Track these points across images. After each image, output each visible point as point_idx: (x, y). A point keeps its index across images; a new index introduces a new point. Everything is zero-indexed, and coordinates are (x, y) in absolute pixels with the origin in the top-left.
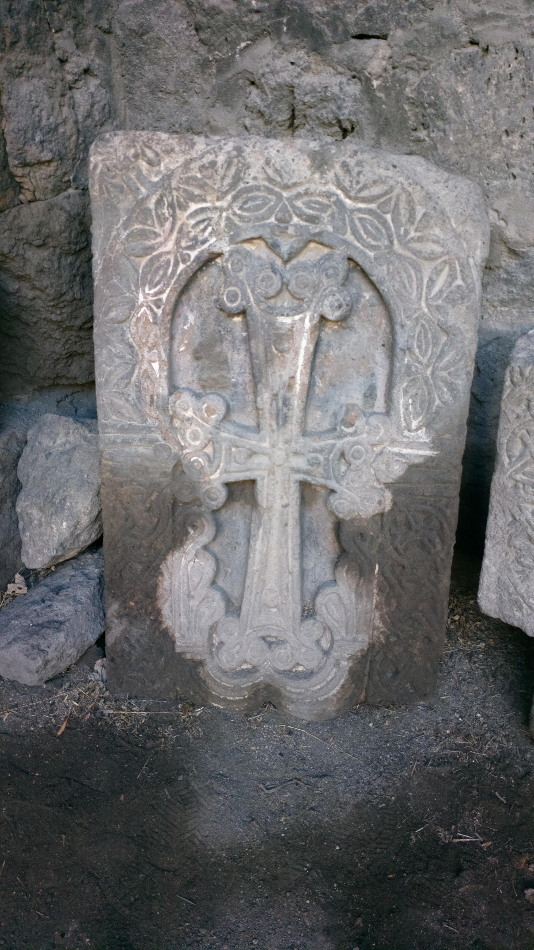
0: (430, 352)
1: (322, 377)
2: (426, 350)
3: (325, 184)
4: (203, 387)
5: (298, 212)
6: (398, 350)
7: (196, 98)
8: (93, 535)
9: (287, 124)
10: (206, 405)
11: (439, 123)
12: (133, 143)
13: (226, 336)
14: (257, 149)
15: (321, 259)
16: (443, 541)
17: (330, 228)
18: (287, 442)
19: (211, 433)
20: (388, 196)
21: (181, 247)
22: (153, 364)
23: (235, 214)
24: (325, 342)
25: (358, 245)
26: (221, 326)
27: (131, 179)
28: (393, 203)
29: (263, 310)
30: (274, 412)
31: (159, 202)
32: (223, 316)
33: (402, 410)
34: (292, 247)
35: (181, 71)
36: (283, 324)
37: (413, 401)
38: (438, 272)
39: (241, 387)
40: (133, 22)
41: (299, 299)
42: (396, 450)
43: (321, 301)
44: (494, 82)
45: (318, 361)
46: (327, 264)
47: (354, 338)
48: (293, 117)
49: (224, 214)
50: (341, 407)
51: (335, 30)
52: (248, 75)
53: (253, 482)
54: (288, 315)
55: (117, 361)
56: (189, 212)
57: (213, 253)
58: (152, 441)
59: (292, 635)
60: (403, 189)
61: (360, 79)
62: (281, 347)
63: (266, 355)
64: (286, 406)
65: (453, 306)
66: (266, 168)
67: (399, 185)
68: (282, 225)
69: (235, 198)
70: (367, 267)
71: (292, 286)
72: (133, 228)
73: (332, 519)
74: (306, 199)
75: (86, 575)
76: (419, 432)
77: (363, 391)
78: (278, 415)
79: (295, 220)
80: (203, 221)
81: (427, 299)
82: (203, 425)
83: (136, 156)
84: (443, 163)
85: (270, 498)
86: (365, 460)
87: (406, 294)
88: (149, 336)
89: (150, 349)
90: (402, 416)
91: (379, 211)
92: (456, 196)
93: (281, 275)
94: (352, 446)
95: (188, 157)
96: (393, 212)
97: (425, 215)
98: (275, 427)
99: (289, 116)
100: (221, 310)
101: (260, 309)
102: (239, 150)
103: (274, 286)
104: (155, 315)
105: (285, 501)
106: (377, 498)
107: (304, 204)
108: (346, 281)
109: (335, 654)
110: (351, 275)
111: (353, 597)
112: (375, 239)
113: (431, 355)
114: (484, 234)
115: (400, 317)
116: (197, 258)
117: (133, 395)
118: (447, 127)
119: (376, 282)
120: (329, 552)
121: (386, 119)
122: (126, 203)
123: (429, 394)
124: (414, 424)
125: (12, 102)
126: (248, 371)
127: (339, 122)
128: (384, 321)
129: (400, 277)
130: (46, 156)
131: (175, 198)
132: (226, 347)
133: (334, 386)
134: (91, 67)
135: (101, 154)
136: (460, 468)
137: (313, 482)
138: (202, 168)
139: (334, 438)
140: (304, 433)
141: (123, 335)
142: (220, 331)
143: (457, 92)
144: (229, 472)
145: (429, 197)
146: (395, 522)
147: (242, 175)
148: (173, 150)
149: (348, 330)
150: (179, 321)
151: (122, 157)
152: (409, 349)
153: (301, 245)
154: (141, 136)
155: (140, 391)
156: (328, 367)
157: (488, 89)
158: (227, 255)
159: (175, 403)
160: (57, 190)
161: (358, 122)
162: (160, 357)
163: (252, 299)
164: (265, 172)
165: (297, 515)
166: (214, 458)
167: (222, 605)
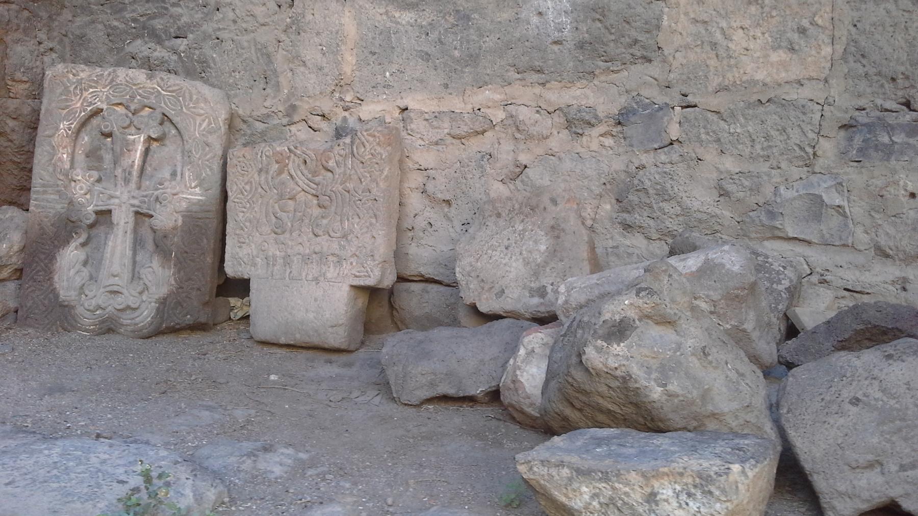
18: (129, 192)
31: (76, 87)
38: (204, 121)
40: (78, 32)
47: (167, 149)
51: (166, 36)
53: (110, 211)
58: (59, 191)
71: (135, 123)
84: (213, 85)
102: (114, 71)
108: (161, 124)
111: (160, 269)
115: (186, 137)
117: (51, 169)
125: (12, 53)
130: (25, 79)
132: (102, 152)
140: (139, 188)
150: (80, 139)
160: (28, 97)
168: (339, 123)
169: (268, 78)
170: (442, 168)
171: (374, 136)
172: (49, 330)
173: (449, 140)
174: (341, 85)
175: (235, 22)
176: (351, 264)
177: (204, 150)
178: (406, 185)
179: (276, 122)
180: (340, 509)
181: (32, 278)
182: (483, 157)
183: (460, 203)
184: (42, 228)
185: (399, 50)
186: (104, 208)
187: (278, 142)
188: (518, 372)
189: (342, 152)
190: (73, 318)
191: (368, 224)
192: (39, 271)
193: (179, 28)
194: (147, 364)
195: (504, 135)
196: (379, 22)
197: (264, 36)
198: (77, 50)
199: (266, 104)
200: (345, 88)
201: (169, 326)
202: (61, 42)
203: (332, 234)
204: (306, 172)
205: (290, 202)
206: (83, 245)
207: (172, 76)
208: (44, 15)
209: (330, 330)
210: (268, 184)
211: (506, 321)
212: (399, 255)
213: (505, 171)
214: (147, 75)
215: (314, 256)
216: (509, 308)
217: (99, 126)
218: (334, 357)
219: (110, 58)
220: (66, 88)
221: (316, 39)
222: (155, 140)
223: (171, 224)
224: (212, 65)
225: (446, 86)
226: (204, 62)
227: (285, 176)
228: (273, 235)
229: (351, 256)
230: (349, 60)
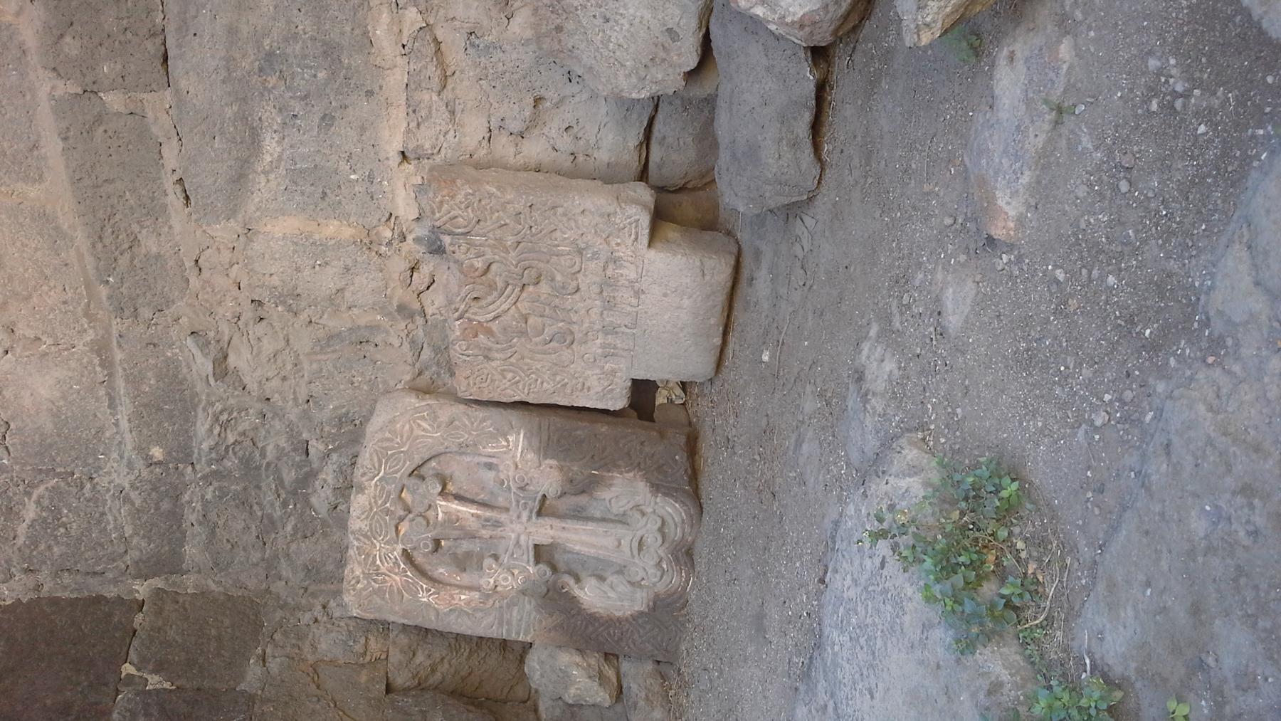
1: (477, 494)
3: (371, 487)
18: (511, 522)
31: (375, 581)
40: (302, 575)
47: (457, 473)
53: (536, 546)
58: (508, 606)
70: (414, 466)
71: (422, 510)
84: (371, 412)
102: (353, 533)
115: (442, 449)
130: (363, 640)
132: (459, 551)
140: (507, 510)
146: (565, 460)
160: (386, 637)
168: (423, 249)
169: (362, 340)
170: (488, 106)
171: (442, 202)
172: (683, 625)
173: (447, 94)
174: (369, 243)
175: (284, 379)
176: (618, 244)
177: (457, 428)
178: (512, 160)
179: (421, 333)
180: (951, 290)
181: (617, 642)
182: (472, 45)
183: (538, 84)
184: (555, 627)
185: (318, 159)
186: (532, 553)
187: (449, 332)
188: (789, 20)
189: (463, 248)
191: (565, 219)
192: (609, 634)
193: (294, 450)
194: (735, 511)
195: (442, 12)
196: (279, 184)
197: (303, 343)
198: (326, 576)
199: (396, 343)
200: (374, 238)
201: (688, 482)
202: (314, 595)
203: (577, 268)
204: (490, 299)
205: (531, 321)
206: (578, 580)
207: (360, 461)
208: (279, 614)
209: (708, 278)
210: (504, 349)
211: (712, 28)
212: (608, 177)
213: (494, 13)
214: (358, 493)
215: (605, 294)
216: (694, 23)
217: (425, 555)
218: (745, 273)
219: (336, 537)
220: (375, 592)
221: (307, 272)
222: (444, 486)
224: (344, 410)
225: (370, 93)
227: (495, 326)
228: (574, 346)
229: (608, 244)
230: (332, 229)
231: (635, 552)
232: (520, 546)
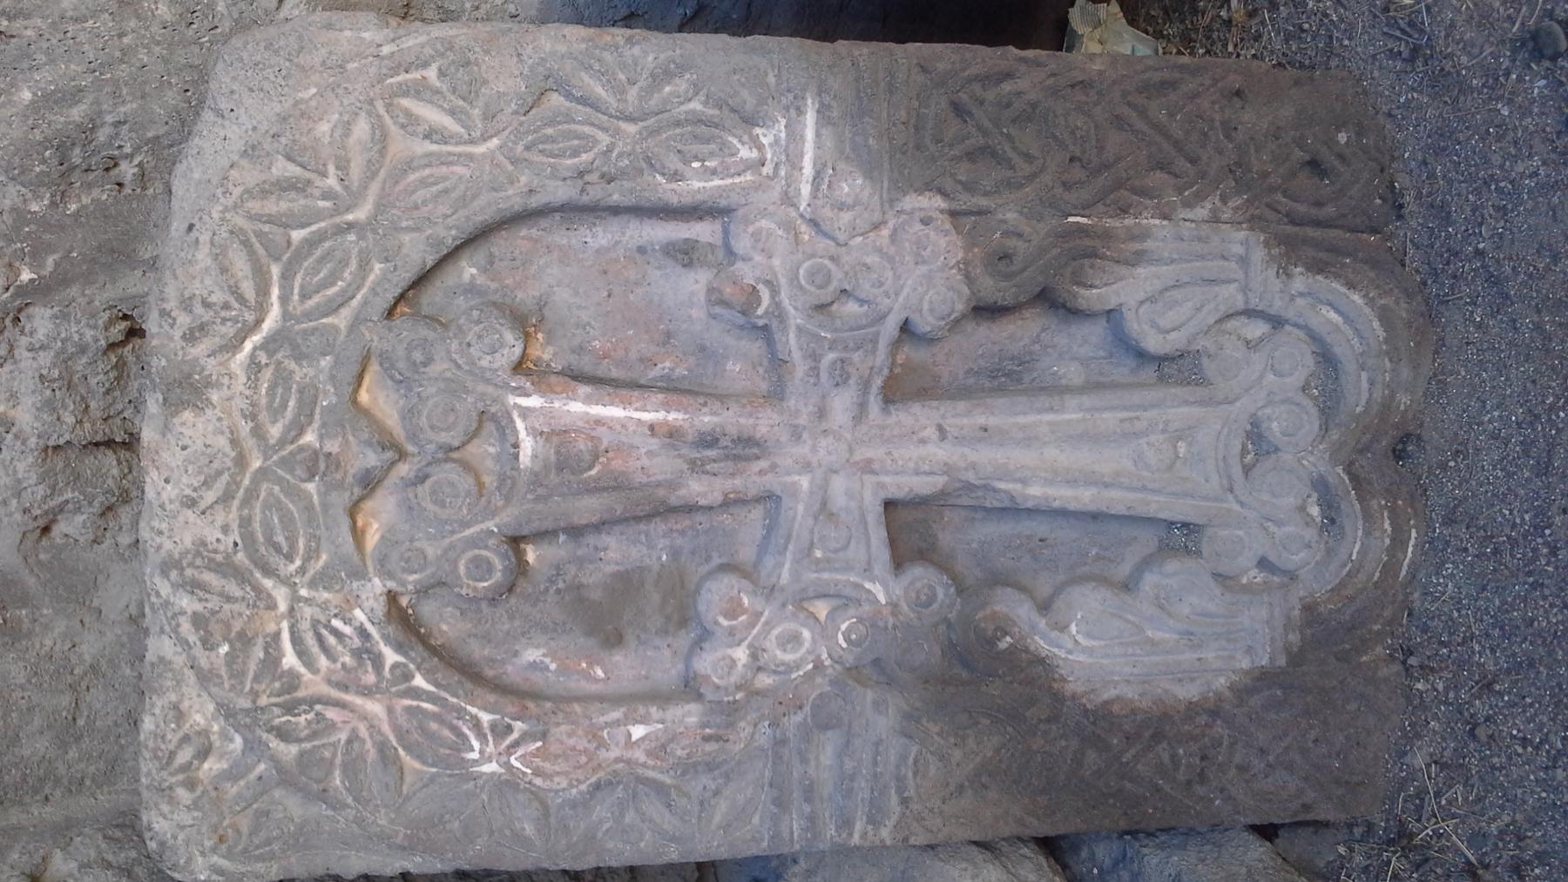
0: (587, 129)
2: (578, 137)
4: (683, 623)
5: (293, 433)
6: (585, 199)
7: (84, 648)
8: (1025, 851)
9: (123, 454)
10: (721, 620)
11: (102, 135)
12: (166, 792)
13: (568, 578)
14: (164, 526)
15: (392, 378)
16: (1009, 75)
17: (326, 362)
18: (796, 434)
19: (784, 605)
20: (254, 240)
21: (377, 686)
22: (634, 738)
23: (302, 570)
24: (573, 359)
25: (359, 297)
26: (547, 590)
27: (239, 795)
28: (266, 228)
29: (508, 499)
30: (729, 466)
31: (284, 734)
32: (523, 586)
33: (717, 182)
34: (368, 443)
35: (29, 681)
36: (535, 456)
37: (696, 158)
38: (410, 123)
39: (679, 541)
41: (480, 422)
42: (806, 190)
43: (483, 376)
44: (5, 23)
45: (615, 373)
46: (401, 365)
47: (562, 296)
48: (109, 443)
49: (304, 592)
50: (714, 317)
52: (29, 543)
53: (889, 505)
54: (516, 446)
55: (630, 817)
56: (303, 670)
57: (388, 614)
59: (1238, 404)
60: (236, 206)
61: (20, 310)
62: (588, 457)
63: (605, 489)
64: (717, 440)
65: (485, 82)
66: (203, 505)
67: (228, 216)
68: (322, 466)
69: (269, 571)
70: (407, 276)
72: (341, 788)
73: (969, 326)
74: (263, 417)
75: (1116, 864)
76: (765, 141)
77: (679, 269)
78: (737, 458)
79: (310, 438)
80: (320, 639)
81: (472, 142)
82: (766, 623)
83: (191, 785)
84: (184, 124)
85: (926, 468)
86: (832, 258)
87: (462, 187)
88: (573, 749)
89: (602, 744)
90: (729, 181)
91: (285, 258)
92: (251, 90)
93: (429, 464)
94: (801, 288)
95: (190, 676)
96: (286, 226)
97: (289, 158)
98: (763, 464)
99: (109, 453)
100: (511, 590)
101: (505, 507)
103: (454, 477)
104: (525, 738)
105: (931, 432)
106: (918, 227)
107: (274, 423)
109: (1278, 306)
110: (425, 310)
111: (1140, 270)
112: (344, 263)
113: (592, 124)
114: (329, 26)
115: (512, 198)
116: (399, 648)
117: (705, 780)
118: (109, 119)
119: (438, 256)
120: (1044, 330)
121: (99, 249)
122: (293, 806)
123: (678, 124)
124: (746, 153)
126: (642, 527)
127: (112, 346)
128: (524, 232)
129: (425, 203)
131: (274, 700)
132: (593, 578)
133: (669, 335)
134: (27, 871)
135: (189, 860)
136: (842, 45)
137: (886, 372)
138: (208, 645)
139: (785, 330)
140: (776, 395)
141: (574, 805)
142: (558, 591)
143: (32, 102)
144: (869, 563)
145: (251, 151)
146: (969, 188)
147: (219, 558)
148: (175, 707)
149: (546, 312)
151: (196, 814)
152: (581, 174)
153: (363, 422)
154: (149, 774)
155: (695, 765)
156: (627, 350)
157: (19, 36)
158: (391, 584)
159: (718, 687)
161: (111, 307)
162: (617, 723)
163: (483, 526)
164: (211, 507)
165: (962, 406)
166: (838, 596)
167: (1172, 565)
186: (878, 535)
190: (1351, 599)
214: (173, 405)
223: (944, 244)
224: (77, 113)
226: (63, 150)
231: (1237, 471)
232: (831, 515)
